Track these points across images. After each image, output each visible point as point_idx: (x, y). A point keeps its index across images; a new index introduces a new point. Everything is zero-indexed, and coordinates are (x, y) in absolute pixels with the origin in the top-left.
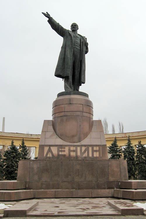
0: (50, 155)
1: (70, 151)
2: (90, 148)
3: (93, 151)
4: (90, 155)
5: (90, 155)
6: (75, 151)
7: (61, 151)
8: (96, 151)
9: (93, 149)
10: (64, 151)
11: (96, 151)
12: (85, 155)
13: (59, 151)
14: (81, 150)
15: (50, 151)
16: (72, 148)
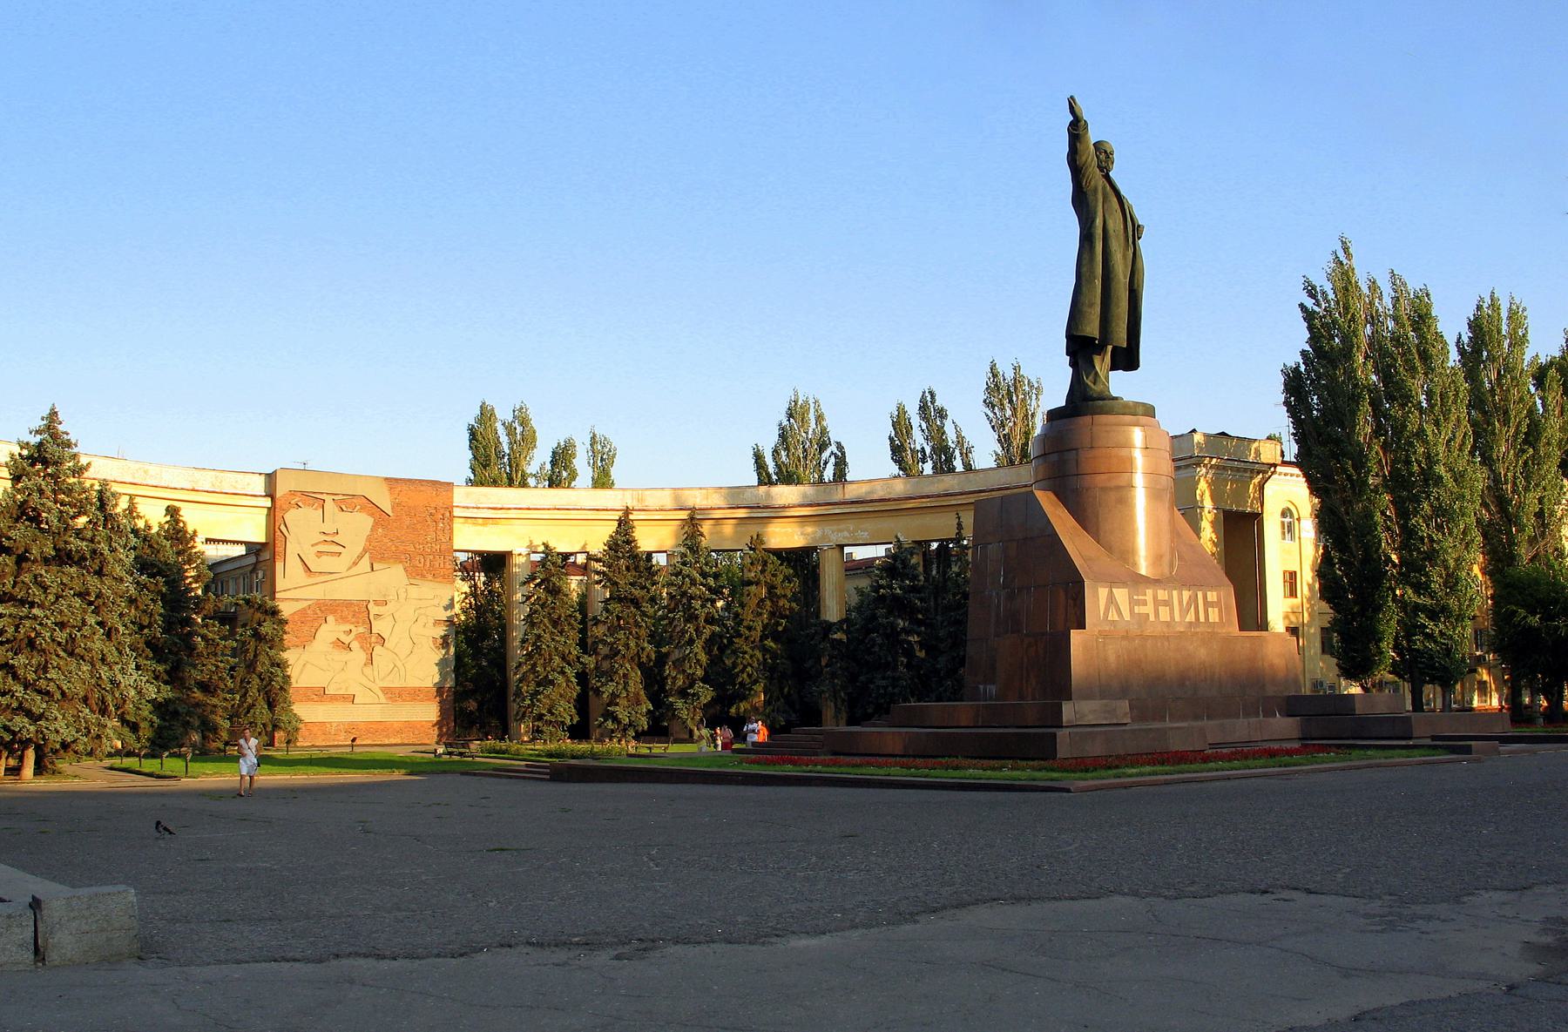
0: (1113, 616)
1: (1157, 603)
2: (1200, 595)
3: (1207, 604)
4: (1202, 619)
5: (1202, 619)
6: (1168, 603)
7: (1139, 603)
8: (1212, 604)
9: (1205, 597)
10: (1145, 603)
11: (1212, 604)
12: (1190, 617)
13: (1133, 603)
14: (1181, 602)
15: (1111, 599)
16: (1162, 594)
